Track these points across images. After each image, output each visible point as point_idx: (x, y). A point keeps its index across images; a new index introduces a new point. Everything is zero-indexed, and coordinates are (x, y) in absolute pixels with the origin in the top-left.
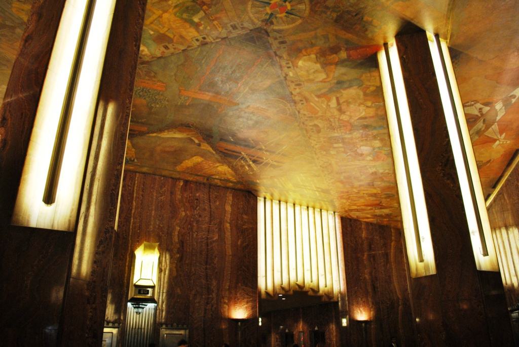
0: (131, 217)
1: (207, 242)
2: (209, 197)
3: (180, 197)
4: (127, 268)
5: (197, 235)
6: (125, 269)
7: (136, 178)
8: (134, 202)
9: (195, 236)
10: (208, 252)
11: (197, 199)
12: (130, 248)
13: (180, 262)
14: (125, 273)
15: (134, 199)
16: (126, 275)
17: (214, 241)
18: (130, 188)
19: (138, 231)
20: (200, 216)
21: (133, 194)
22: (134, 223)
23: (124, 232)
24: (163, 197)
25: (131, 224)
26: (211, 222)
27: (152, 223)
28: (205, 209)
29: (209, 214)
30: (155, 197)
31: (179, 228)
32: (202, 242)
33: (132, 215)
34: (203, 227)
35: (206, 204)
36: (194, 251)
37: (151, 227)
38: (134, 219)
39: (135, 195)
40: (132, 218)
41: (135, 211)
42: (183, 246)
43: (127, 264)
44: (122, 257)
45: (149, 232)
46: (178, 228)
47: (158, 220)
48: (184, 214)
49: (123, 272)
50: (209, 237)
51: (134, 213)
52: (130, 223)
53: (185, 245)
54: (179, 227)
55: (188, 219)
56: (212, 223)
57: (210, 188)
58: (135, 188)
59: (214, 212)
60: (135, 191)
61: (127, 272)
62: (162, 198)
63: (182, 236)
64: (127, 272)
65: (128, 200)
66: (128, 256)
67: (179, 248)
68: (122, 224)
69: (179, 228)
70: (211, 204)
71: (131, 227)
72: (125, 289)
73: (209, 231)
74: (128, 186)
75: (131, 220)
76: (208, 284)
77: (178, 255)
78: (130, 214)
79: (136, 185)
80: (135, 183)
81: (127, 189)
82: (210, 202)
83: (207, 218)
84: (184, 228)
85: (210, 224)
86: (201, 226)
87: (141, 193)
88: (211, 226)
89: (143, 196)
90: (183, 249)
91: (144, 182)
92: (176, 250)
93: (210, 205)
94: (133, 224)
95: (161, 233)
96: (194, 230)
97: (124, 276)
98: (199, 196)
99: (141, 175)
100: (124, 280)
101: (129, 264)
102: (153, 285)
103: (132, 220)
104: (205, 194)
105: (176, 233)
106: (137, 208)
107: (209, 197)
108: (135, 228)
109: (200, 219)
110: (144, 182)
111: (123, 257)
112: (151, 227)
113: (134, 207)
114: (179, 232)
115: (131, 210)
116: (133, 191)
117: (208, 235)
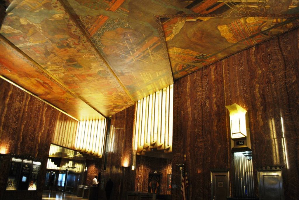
0: (224, 91)
1: (286, 87)
2: (280, 47)
3: (255, 60)
4: (227, 128)
5: (275, 85)
6: (226, 129)
7: (223, 64)
8: (224, 80)
9: (273, 86)
10: (288, 96)
11: (269, 55)
12: (227, 113)
13: (264, 112)
14: (227, 131)
15: (224, 79)
16: (227, 133)
17: (293, 84)
18: (220, 72)
19: (230, 99)
20: (275, 67)
21: (223, 75)
22: (227, 95)
23: (222, 104)
24: (242, 67)
25: (225, 96)
26: (286, 68)
27: (238, 90)
28: (278, 59)
29: (283, 62)
30: (237, 70)
31: (259, 85)
32: (281, 89)
33: (225, 90)
34: (280, 75)
35: (278, 54)
36: (275, 99)
37: (238, 93)
38: (226, 92)
39: (224, 75)
40: (225, 92)
41: (226, 87)
42: (264, 99)
43: (227, 125)
44: (223, 121)
45: (237, 97)
46: (258, 86)
47: (242, 86)
48: (260, 72)
49: (225, 132)
50: (286, 82)
51: (226, 88)
52: (224, 96)
53: (266, 97)
54: (259, 84)
55: (265, 74)
56: (287, 68)
57: (278, 39)
58: (223, 70)
59: (287, 58)
60: (224, 72)
61: (227, 131)
62: (242, 68)
63: (263, 90)
64: (227, 131)
65: (221, 81)
66: (226, 119)
67: (261, 101)
68: (219, 98)
69: (259, 85)
70: (283, 52)
71: (225, 98)
72: (228, 143)
73: (285, 77)
74: (219, 71)
75: (224, 93)
76: (294, 125)
77: (262, 107)
78: (224, 90)
79: (224, 68)
80: (222, 67)
81: (219, 74)
82: (281, 51)
83: (281, 66)
84: (262, 84)
85: (286, 70)
86: (277, 75)
87: (227, 72)
88: (286, 71)
89: (229, 74)
90: (265, 101)
91: (228, 64)
92: (259, 103)
93: (282, 53)
94: (226, 96)
95: (245, 95)
96: (272, 81)
97: (226, 134)
98: (270, 51)
99: (225, 60)
100: (226, 136)
101: (228, 125)
102: (244, 136)
103: (225, 93)
104: (275, 47)
105: (257, 90)
106: (226, 84)
107: (280, 47)
108: (228, 98)
109: (276, 69)
110: (228, 64)
111: (224, 121)
112: (238, 93)
113: (225, 84)
114: (259, 88)
115: (224, 87)
116: (223, 73)
117: (286, 81)
